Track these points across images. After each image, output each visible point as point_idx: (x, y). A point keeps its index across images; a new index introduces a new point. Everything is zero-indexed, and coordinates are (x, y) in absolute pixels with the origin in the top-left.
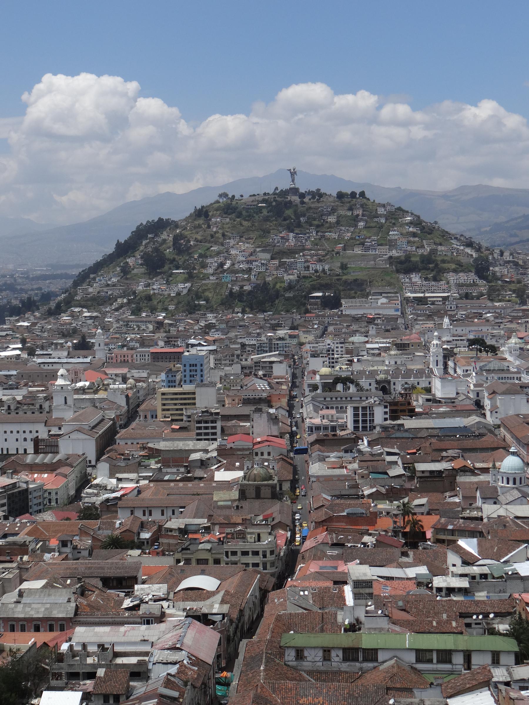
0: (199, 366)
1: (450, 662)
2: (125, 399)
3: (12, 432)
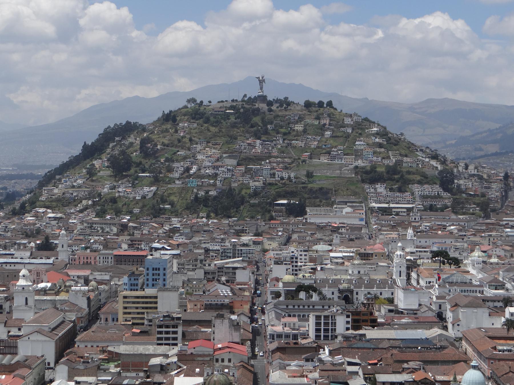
0: (161, 269)
2: (86, 301)
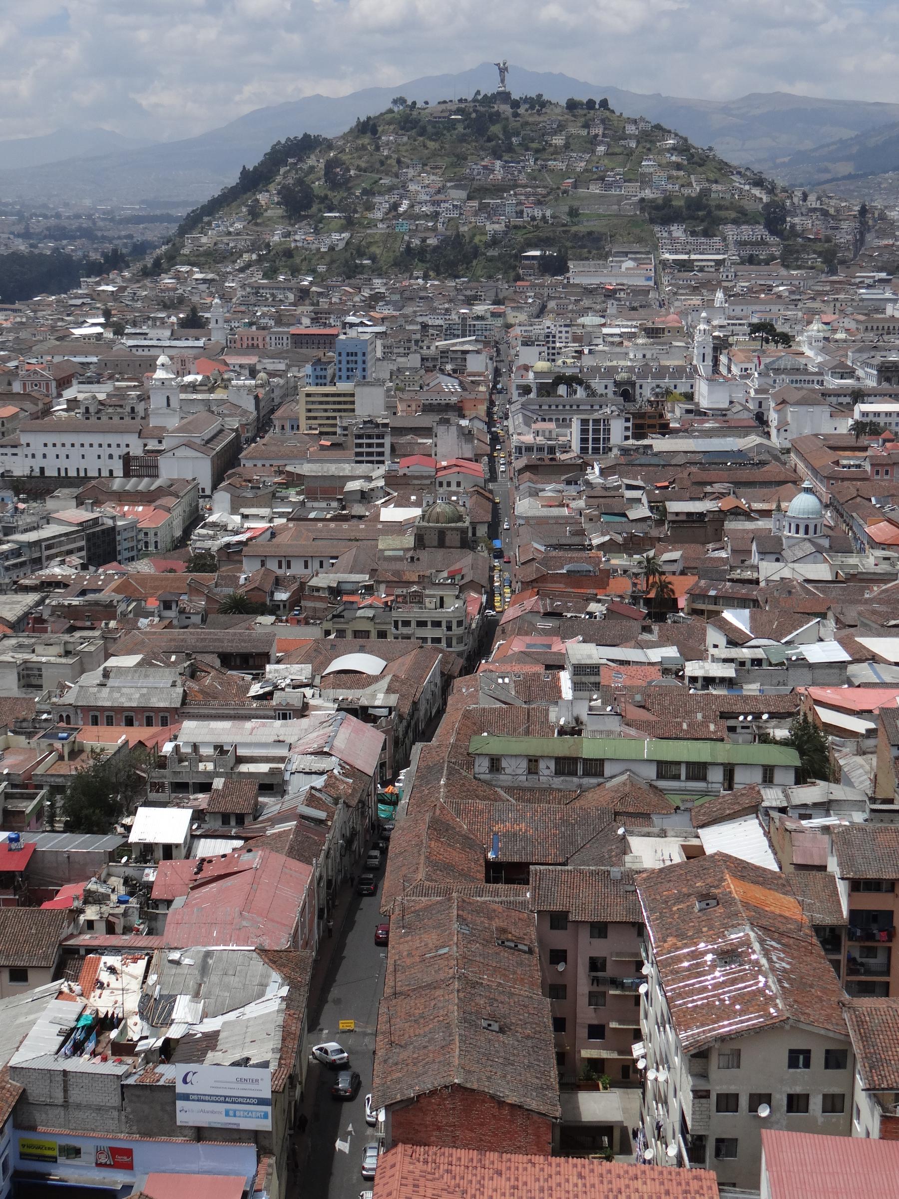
1: (704, 779)
2: (253, 402)
3: (91, 445)
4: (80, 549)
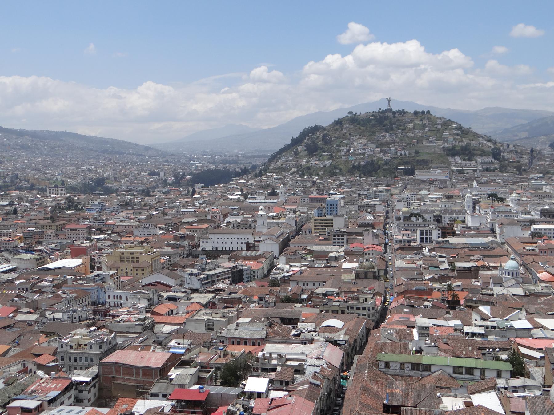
1: (472, 374)
4: (229, 277)
